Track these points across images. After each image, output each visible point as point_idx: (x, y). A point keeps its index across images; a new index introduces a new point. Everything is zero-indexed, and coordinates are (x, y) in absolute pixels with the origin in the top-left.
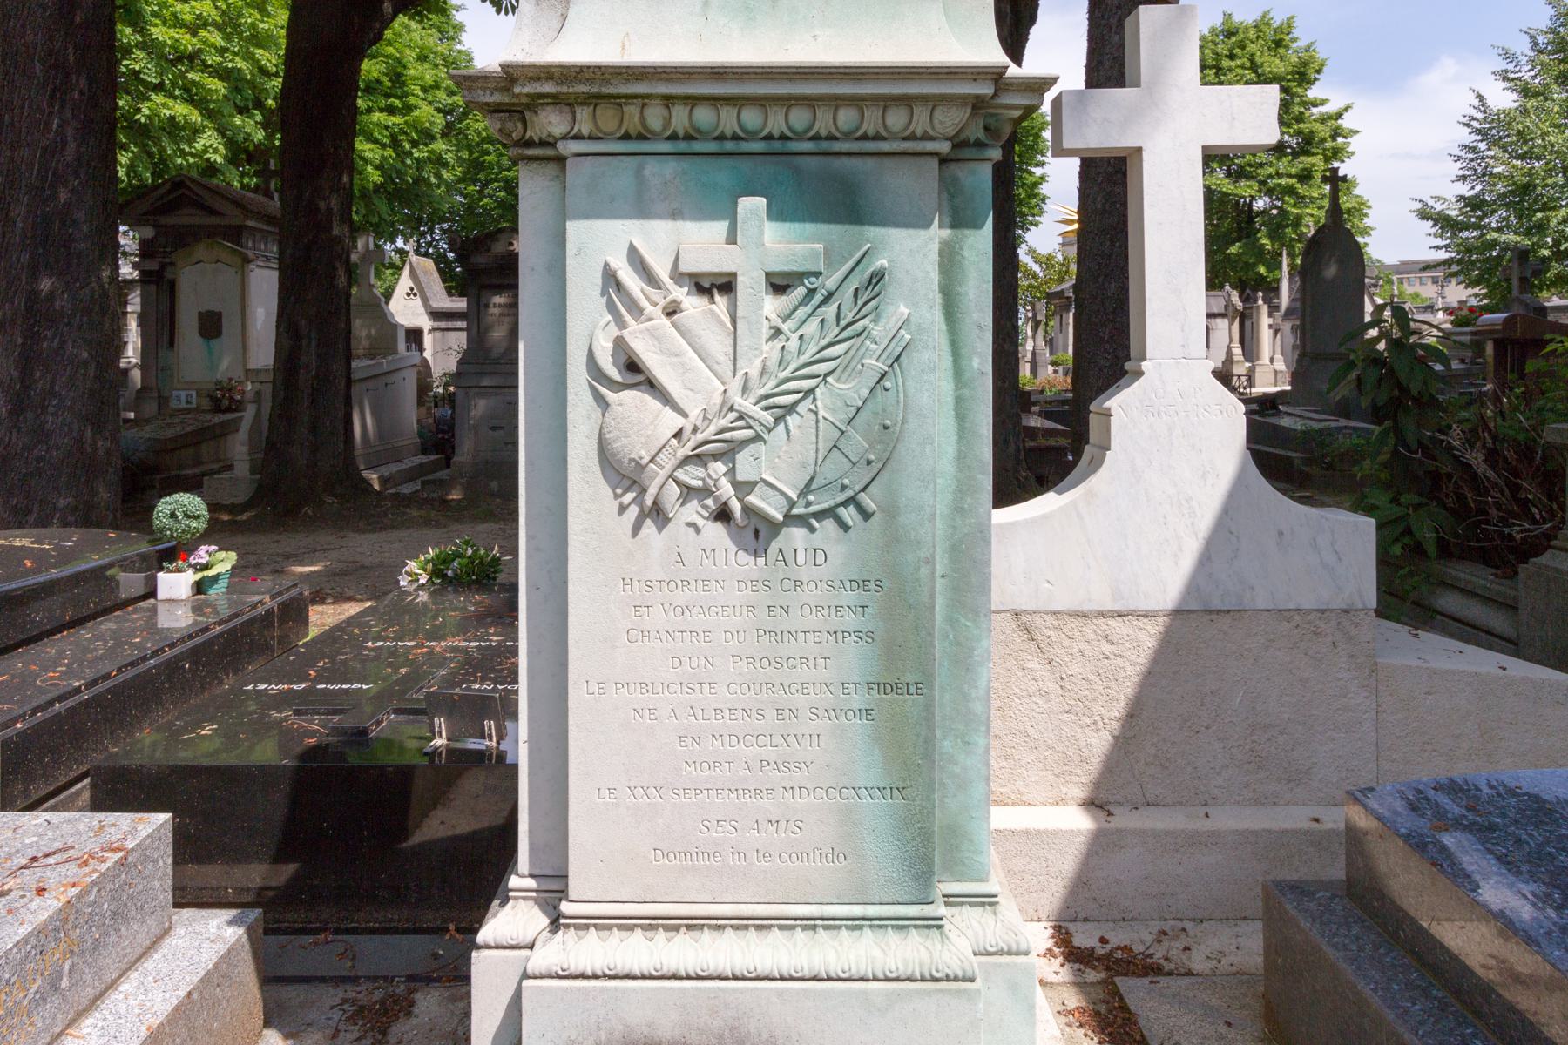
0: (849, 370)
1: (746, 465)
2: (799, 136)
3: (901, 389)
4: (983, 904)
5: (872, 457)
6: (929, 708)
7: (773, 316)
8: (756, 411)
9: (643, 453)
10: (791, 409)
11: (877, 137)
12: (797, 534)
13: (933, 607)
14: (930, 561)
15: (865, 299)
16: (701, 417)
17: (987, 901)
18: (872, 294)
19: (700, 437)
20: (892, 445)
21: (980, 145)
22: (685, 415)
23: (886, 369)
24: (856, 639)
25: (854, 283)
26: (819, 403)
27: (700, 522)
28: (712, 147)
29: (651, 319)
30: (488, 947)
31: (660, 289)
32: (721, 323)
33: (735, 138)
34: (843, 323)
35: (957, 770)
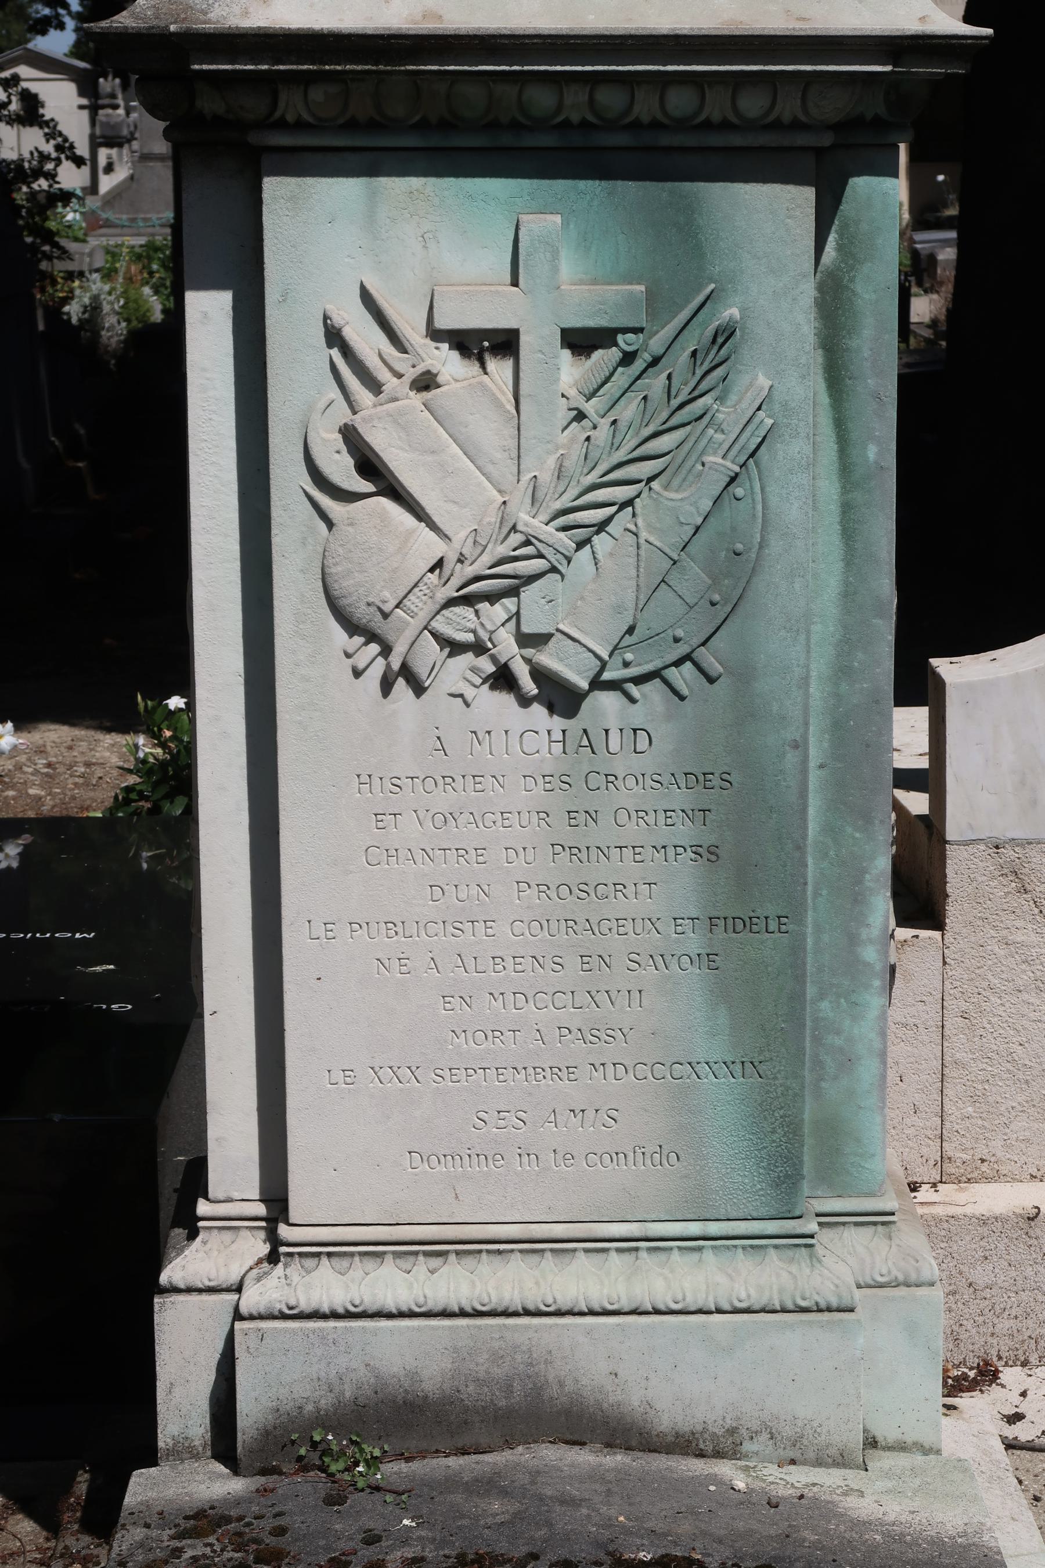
0: (684, 471)
3: (759, 497)
4: (875, 1224)
5: (716, 597)
6: (797, 950)
7: (572, 392)
8: (549, 532)
9: (386, 594)
10: (601, 526)
11: (725, 126)
12: (608, 701)
13: (804, 810)
14: (799, 745)
15: (706, 366)
16: (470, 540)
18: (717, 360)
19: (470, 571)
20: (745, 580)
21: (878, 124)
22: (445, 537)
23: (737, 469)
24: (693, 856)
25: (690, 342)
26: (640, 521)
27: (469, 692)
29: (395, 399)
30: (176, 1290)
31: (406, 352)
32: (499, 405)
33: (515, 126)
34: (675, 403)
35: (838, 1041)
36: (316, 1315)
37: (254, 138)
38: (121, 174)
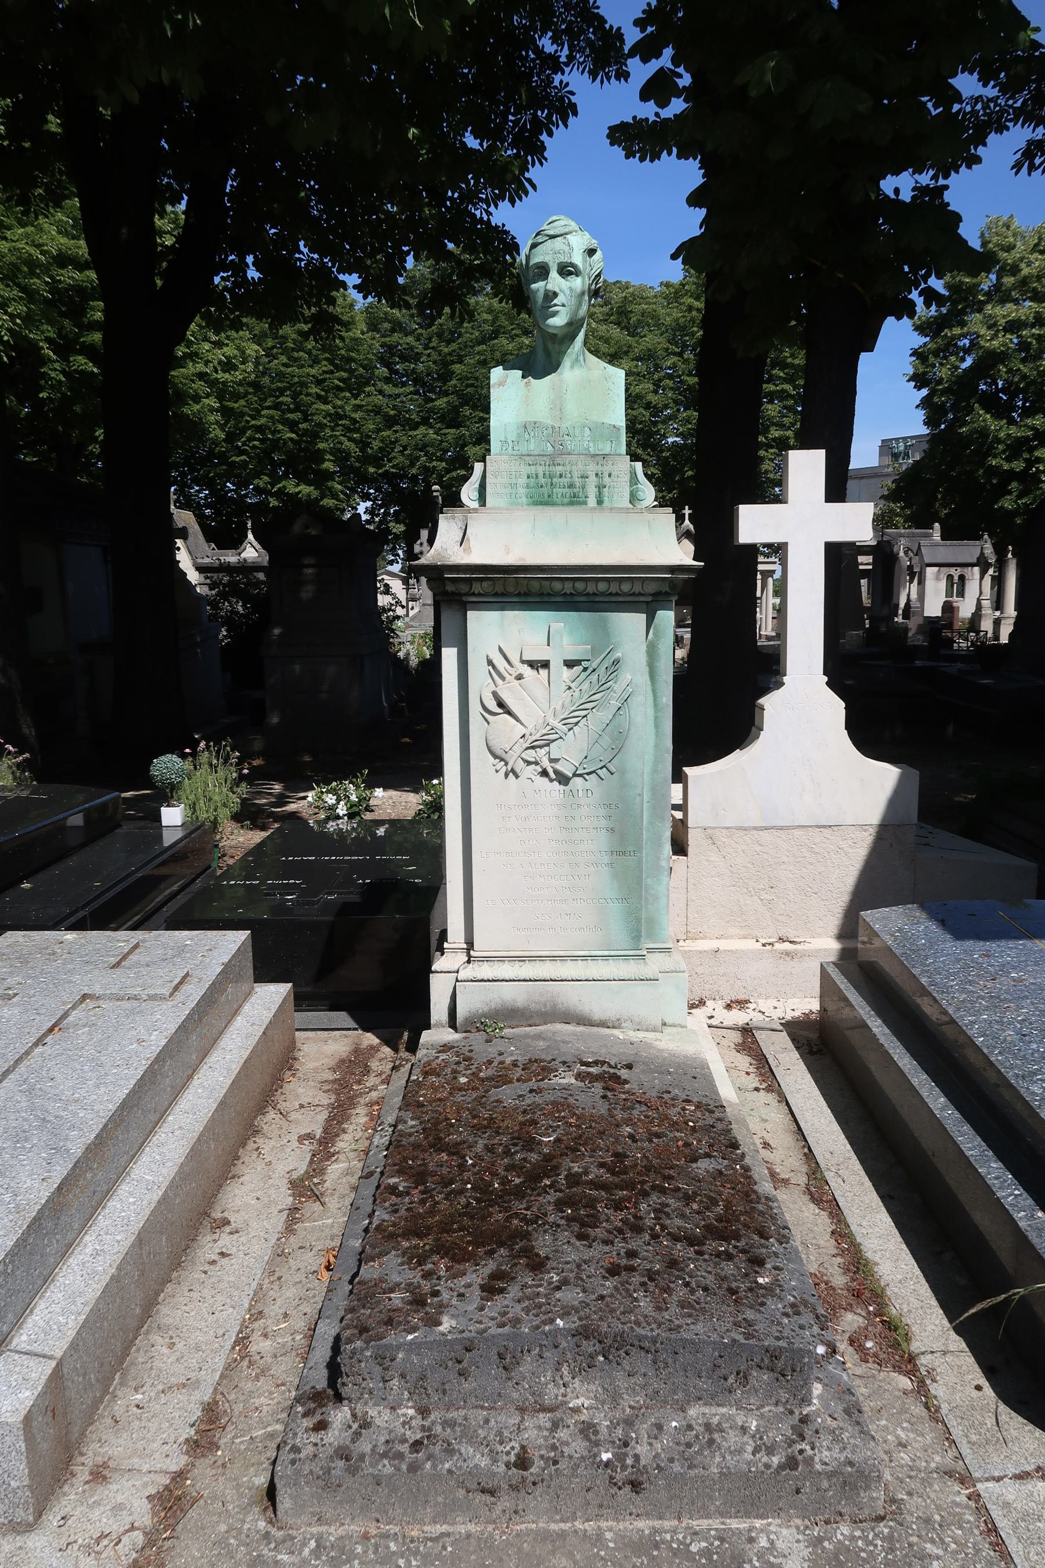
1: (555, 750)
2: (580, 594)
8: (559, 726)
10: (576, 724)
11: (617, 594)
12: (578, 781)
17: (667, 950)
19: (534, 738)
25: (605, 664)
27: (533, 778)
28: (538, 599)
33: (549, 595)
35: (653, 892)
36: (482, 980)
37: (464, 599)
38: (416, 610)
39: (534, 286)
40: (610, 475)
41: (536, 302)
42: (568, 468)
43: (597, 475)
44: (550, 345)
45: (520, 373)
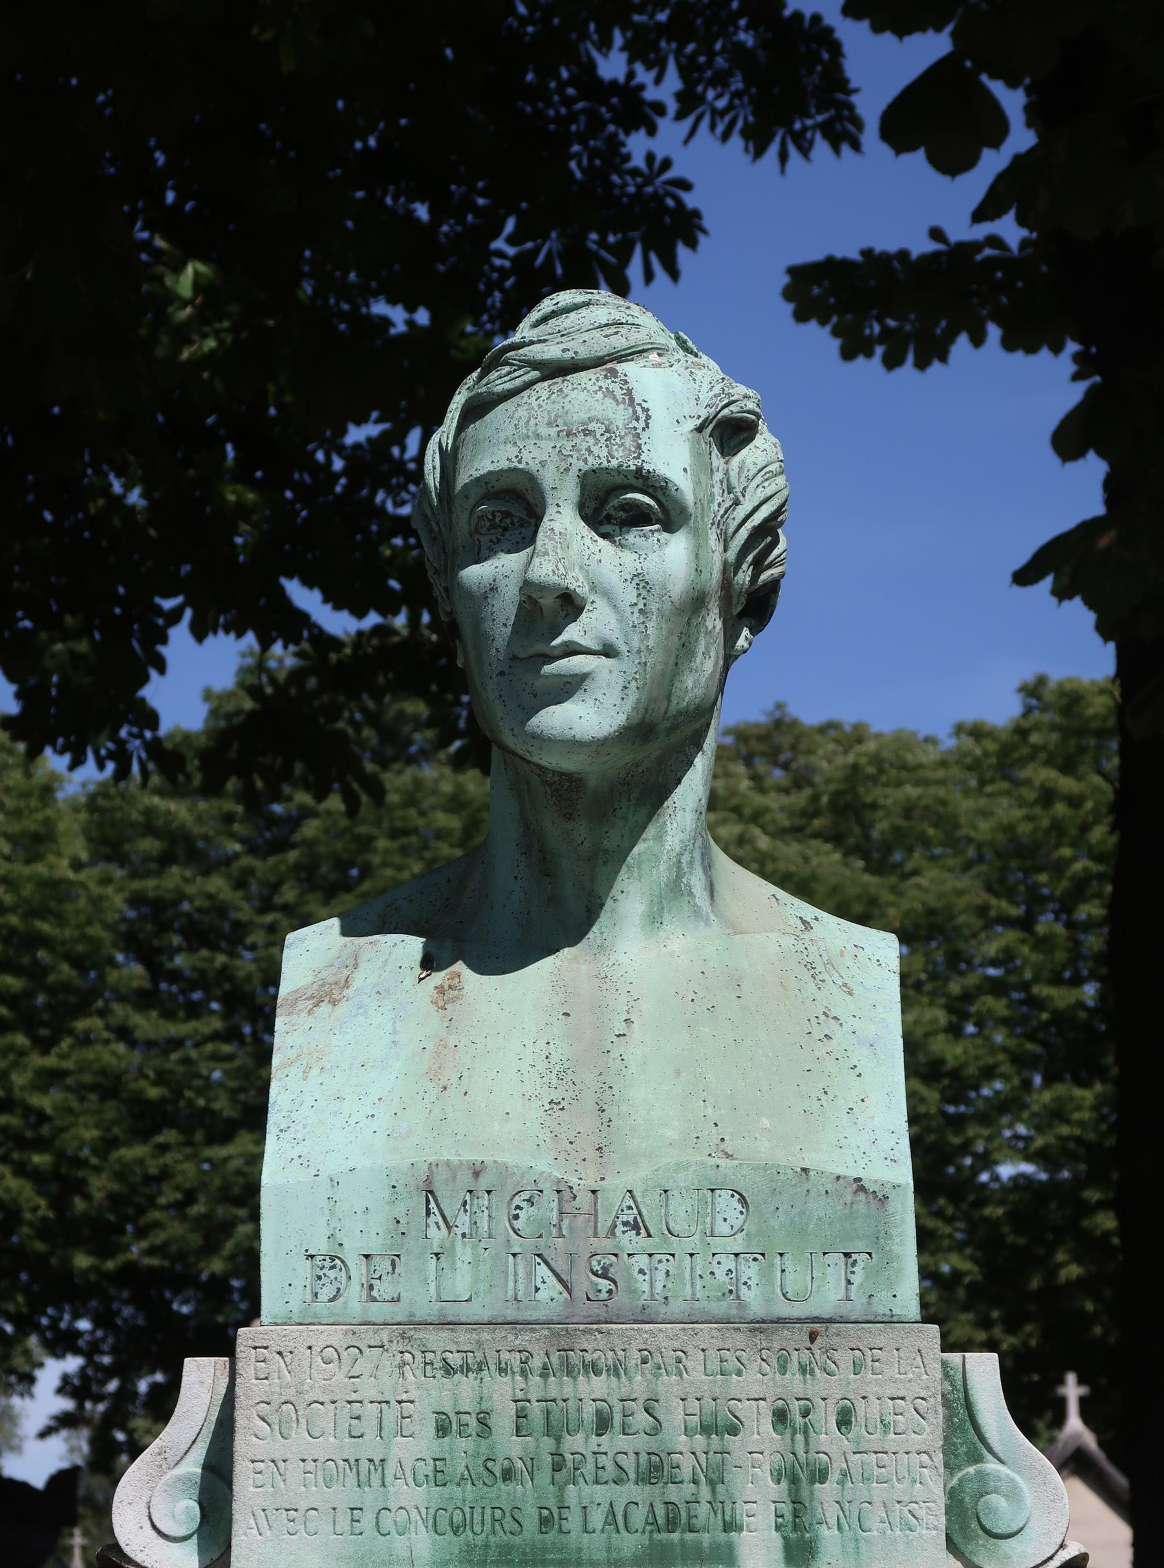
39: (475, 574)
40: (844, 1420)
41: (482, 638)
42: (639, 1385)
43: (781, 1417)
44: (550, 825)
45: (413, 946)
